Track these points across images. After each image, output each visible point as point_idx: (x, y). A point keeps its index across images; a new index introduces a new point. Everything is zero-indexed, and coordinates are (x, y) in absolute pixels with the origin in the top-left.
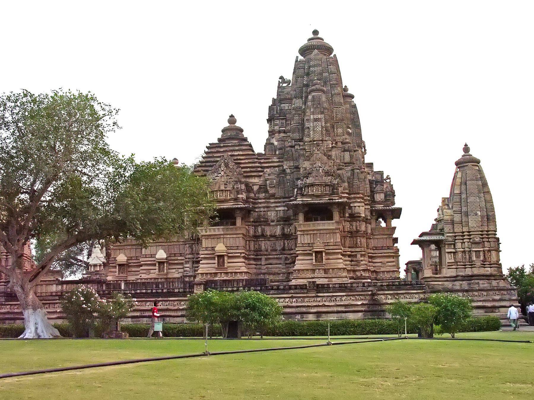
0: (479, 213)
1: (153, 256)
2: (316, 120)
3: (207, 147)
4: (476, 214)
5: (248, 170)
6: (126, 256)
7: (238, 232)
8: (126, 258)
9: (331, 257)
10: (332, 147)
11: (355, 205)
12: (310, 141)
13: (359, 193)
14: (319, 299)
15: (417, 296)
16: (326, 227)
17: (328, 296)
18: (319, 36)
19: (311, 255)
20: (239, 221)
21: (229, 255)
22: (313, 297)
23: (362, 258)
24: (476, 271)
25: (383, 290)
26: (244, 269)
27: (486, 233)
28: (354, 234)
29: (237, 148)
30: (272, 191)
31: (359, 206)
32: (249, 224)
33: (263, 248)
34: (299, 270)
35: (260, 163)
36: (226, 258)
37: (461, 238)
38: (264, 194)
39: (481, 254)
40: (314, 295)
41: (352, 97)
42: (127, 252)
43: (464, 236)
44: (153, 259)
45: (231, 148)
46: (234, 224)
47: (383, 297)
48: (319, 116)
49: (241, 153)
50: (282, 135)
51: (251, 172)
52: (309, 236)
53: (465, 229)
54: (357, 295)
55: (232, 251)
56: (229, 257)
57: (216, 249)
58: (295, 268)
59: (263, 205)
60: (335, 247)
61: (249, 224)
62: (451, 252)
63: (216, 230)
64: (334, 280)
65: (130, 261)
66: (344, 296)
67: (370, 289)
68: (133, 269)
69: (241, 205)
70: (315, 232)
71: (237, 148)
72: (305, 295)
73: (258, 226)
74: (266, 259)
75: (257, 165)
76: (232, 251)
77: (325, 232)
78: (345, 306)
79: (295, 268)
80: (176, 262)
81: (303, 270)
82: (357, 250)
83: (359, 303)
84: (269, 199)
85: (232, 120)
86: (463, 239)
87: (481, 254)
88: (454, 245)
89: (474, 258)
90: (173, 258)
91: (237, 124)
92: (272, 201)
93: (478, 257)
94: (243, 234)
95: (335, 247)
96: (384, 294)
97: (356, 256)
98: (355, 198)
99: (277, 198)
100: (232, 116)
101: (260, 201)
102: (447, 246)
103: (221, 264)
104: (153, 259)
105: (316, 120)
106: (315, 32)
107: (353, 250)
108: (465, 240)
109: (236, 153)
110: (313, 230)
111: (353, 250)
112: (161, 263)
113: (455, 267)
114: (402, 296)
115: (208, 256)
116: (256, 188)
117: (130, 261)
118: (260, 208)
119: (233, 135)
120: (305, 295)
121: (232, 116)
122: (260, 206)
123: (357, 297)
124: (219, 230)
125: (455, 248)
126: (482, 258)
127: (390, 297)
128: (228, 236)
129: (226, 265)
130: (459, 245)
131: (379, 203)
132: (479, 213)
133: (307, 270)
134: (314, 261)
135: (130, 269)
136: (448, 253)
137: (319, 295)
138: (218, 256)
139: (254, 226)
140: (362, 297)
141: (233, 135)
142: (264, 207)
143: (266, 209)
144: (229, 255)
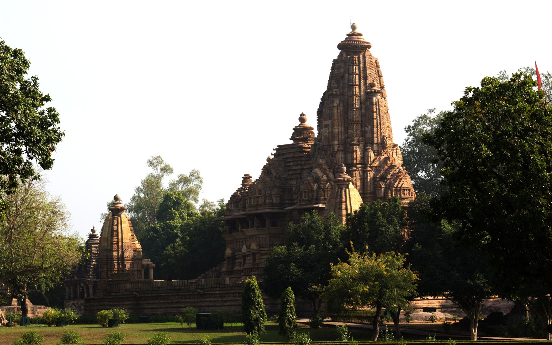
10: (338, 150)
57: (251, 248)
100: (302, 115)
121: (302, 115)
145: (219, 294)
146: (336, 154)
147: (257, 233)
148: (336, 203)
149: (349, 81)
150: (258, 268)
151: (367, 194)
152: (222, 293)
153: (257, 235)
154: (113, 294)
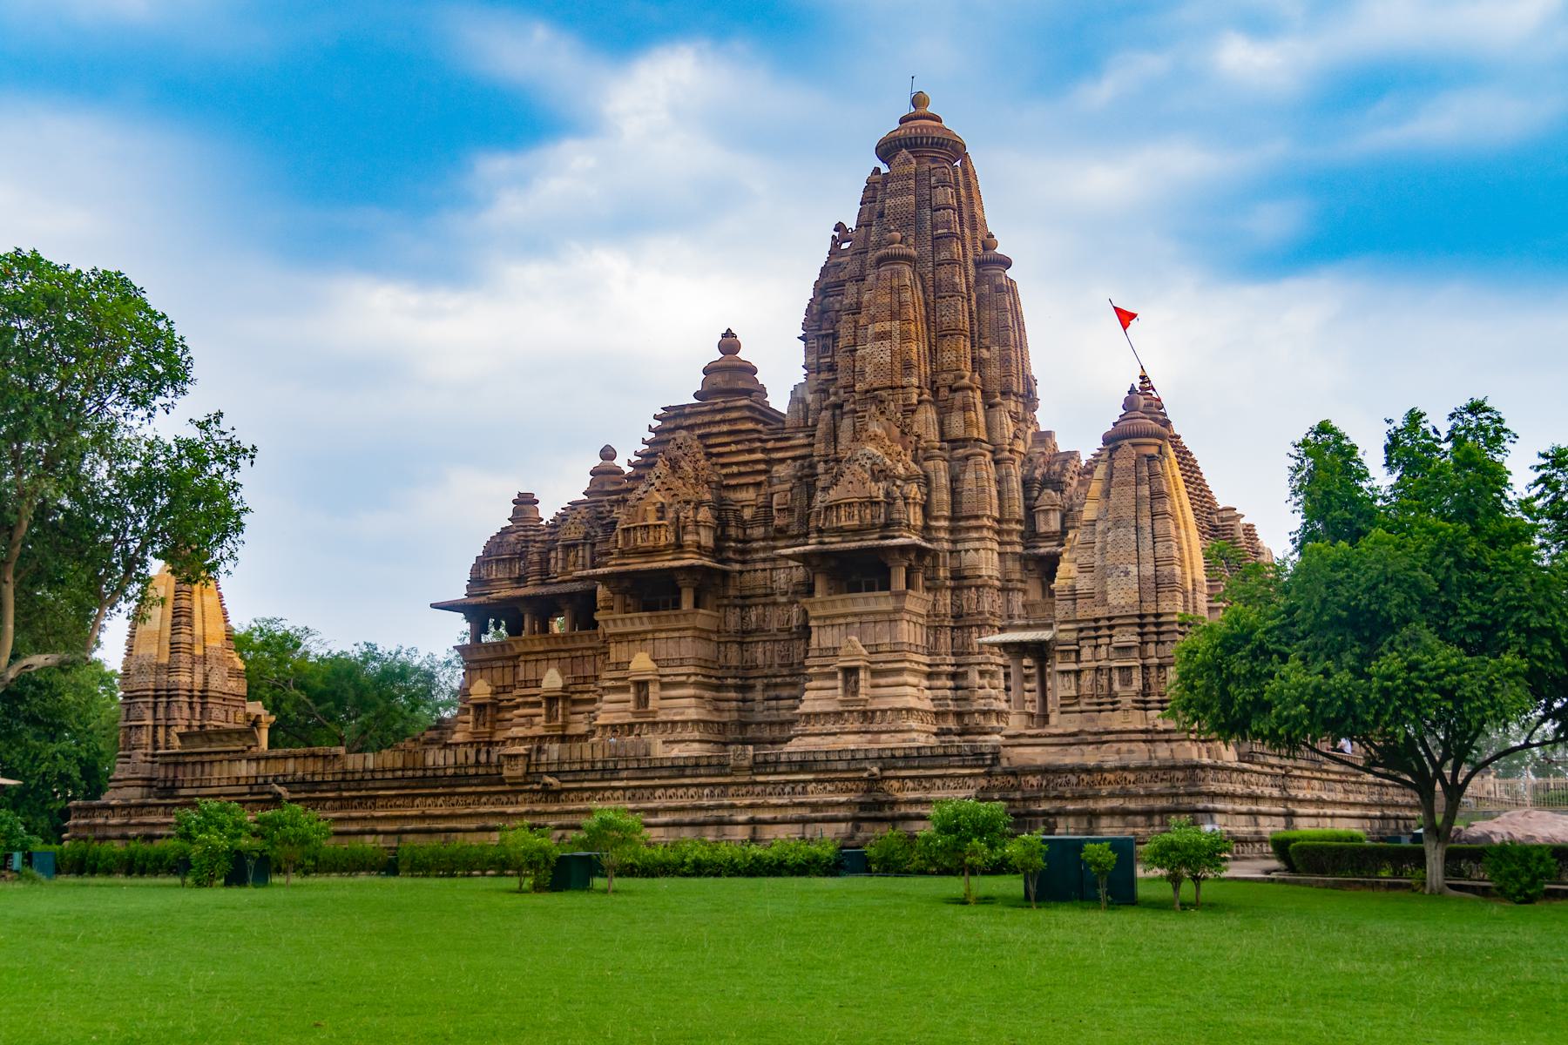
0: (1133, 569)
1: (537, 683)
2: (882, 336)
3: (656, 417)
4: (1127, 573)
5: (735, 469)
6: (492, 683)
7: (683, 624)
8: (489, 689)
9: (882, 681)
10: (920, 402)
11: (968, 545)
12: (867, 391)
13: (977, 517)
14: (758, 789)
15: (971, 782)
16: (873, 607)
17: (776, 783)
18: (929, 110)
19: (833, 675)
21: (665, 680)
22: (746, 784)
23: (985, 682)
24: (1116, 721)
25: (895, 768)
26: (692, 714)
27: (1152, 619)
28: (963, 622)
29: (718, 417)
30: (779, 521)
31: (977, 550)
32: (725, 602)
33: (760, 661)
34: (808, 715)
35: (764, 450)
36: (654, 690)
37: (1093, 633)
38: (762, 530)
39: (1137, 676)
40: (746, 779)
41: (1007, 263)
42: (497, 674)
43: (1144, 625)
44: (535, 691)
45: (707, 419)
46: (677, 604)
47: (896, 784)
48: (887, 326)
49: (725, 428)
50: (824, 376)
51: (740, 474)
52: (836, 630)
53: (1100, 612)
54: (840, 780)
55: (668, 671)
56: (664, 686)
57: (632, 666)
58: (805, 707)
59: (762, 555)
60: (891, 657)
61: (725, 602)
62: (1068, 672)
63: (637, 621)
64: (884, 737)
65: (501, 697)
66: (810, 782)
67: (866, 764)
68: (508, 716)
69: (690, 560)
70: (850, 620)
71: (718, 417)
72: (728, 780)
73: (750, 607)
74: (767, 687)
75: (759, 456)
76: (668, 671)
77: (871, 618)
78: (814, 806)
79: (805, 707)
80: (586, 696)
81: (817, 715)
82: (972, 659)
83: (842, 799)
84: (774, 539)
85: (729, 343)
86: (1096, 638)
87: (1137, 676)
88: (1078, 653)
89: (1117, 687)
90: (580, 688)
91: (742, 355)
93: (1127, 682)
94: (695, 628)
95: (891, 657)
96: (897, 778)
97: (964, 675)
98: (968, 529)
99: (792, 537)
100: (729, 334)
101: (755, 545)
102: (1058, 657)
103: (642, 701)
104: (535, 691)
105: (882, 336)
106: (918, 100)
107: (962, 660)
108: (1100, 641)
109: (715, 429)
110: (844, 616)
111: (962, 660)
112: (551, 701)
113: (1076, 708)
114: (939, 782)
115: (619, 683)
116: (747, 514)
117: (501, 697)
118: (755, 561)
119: (730, 376)
120: (728, 780)
121: (729, 334)
122: (755, 556)
123: (840, 785)
124: (641, 622)
125: (1078, 661)
126: (1137, 684)
127: (910, 784)
128: (664, 635)
129: (652, 705)
130: (1086, 653)
131: (1048, 537)
132: (1133, 569)
133: (827, 714)
134: (840, 691)
135: (500, 716)
136: (1063, 672)
137: (760, 778)
138: (637, 683)
139: (742, 608)
140: (850, 785)
141: (730, 376)
142: (764, 560)
143: (768, 565)
144: (665, 680)
145: (625, 789)
146: (913, 412)
147: (650, 627)
148: (1138, 500)
149: (934, 227)
150: (655, 724)
151: (1008, 521)
152: (635, 787)
153: (646, 632)
154: (183, 792)
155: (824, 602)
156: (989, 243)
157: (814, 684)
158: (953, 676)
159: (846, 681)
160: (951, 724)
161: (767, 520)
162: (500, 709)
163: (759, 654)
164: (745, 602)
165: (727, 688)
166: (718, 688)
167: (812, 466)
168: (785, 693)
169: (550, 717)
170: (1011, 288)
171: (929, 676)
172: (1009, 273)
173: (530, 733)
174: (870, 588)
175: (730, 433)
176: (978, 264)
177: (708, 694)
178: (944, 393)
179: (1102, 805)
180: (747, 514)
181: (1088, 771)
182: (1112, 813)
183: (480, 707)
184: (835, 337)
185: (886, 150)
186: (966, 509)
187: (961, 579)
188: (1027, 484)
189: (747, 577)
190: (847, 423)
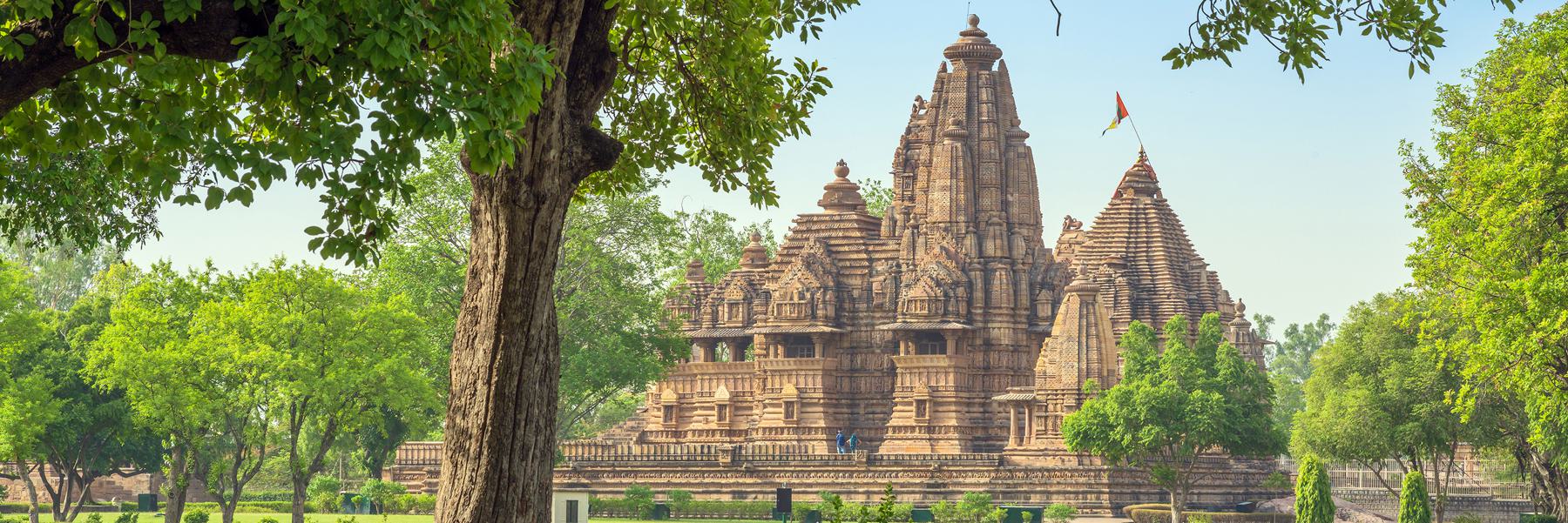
1: (711, 394)
6: (676, 391)
19: (910, 404)
20: (818, 349)
29: (836, 226)
35: (866, 251)
45: (829, 225)
58: (891, 423)
74: (867, 406)
92: (878, 315)
100: (842, 163)
112: (722, 407)
121: (842, 163)
124: (791, 363)
155: (905, 356)
156: (1015, 122)
157: (899, 407)
158: (983, 405)
159: (918, 408)
160: (979, 434)
161: (870, 299)
162: (681, 410)
163: (864, 384)
164: (853, 350)
165: (842, 406)
166: (836, 406)
167: (898, 266)
168: (878, 409)
169: (721, 418)
170: (1028, 153)
171: (968, 405)
172: (1027, 142)
173: (706, 427)
174: (934, 353)
175: (844, 238)
176: (1007, 138)
177: (831, 410)
178: (982, 225)
179: (1054, 489)
180: (856, 293)
181: (1048, 470)
182: (1058, 493)
183: (668, 408)
184: (914, 178)
185: (953, 54)
186: (994, 302)
187: (988, 345)
188: (1032, 285)
189: (855, 335)
190: (921, 240)
